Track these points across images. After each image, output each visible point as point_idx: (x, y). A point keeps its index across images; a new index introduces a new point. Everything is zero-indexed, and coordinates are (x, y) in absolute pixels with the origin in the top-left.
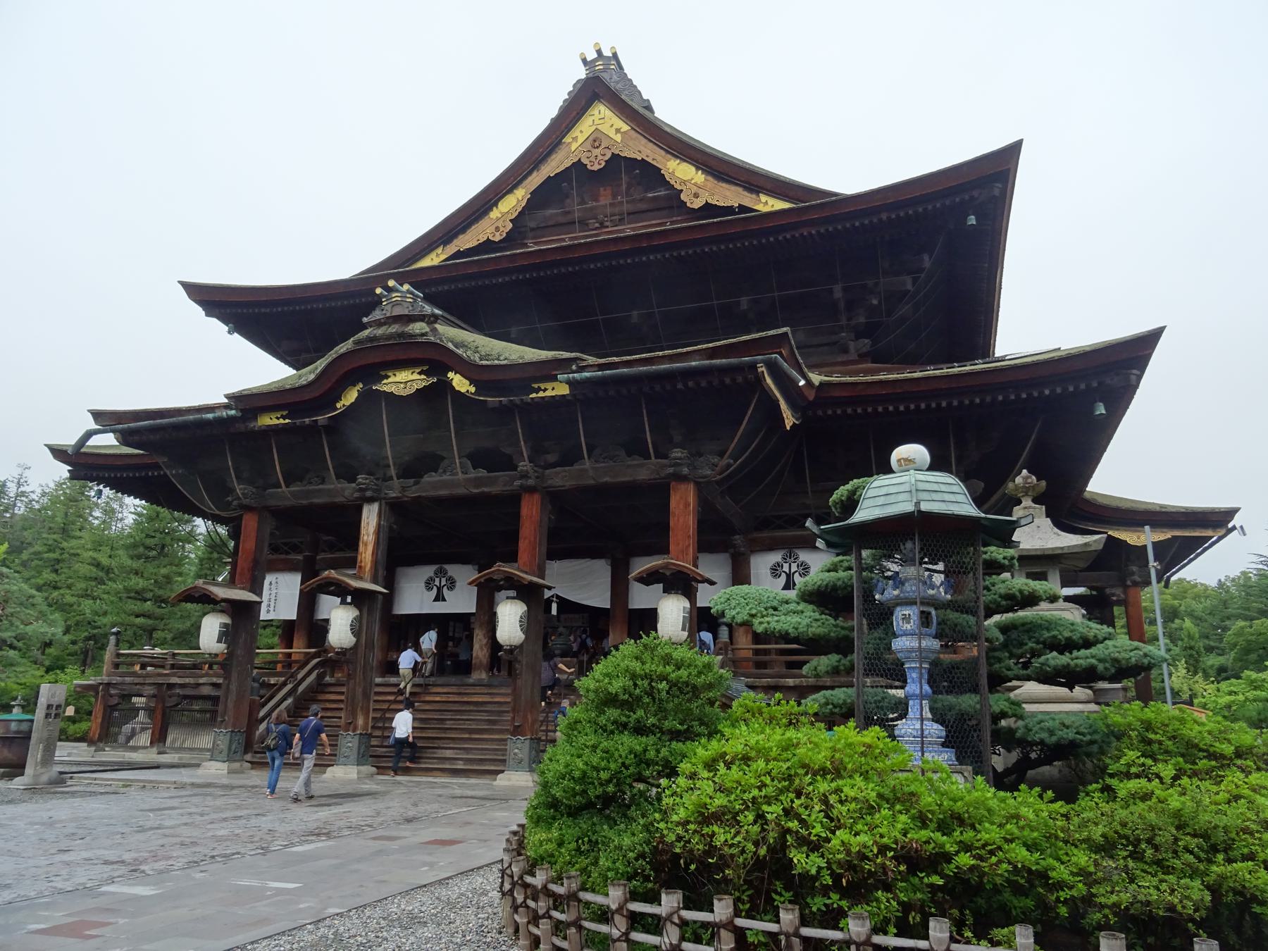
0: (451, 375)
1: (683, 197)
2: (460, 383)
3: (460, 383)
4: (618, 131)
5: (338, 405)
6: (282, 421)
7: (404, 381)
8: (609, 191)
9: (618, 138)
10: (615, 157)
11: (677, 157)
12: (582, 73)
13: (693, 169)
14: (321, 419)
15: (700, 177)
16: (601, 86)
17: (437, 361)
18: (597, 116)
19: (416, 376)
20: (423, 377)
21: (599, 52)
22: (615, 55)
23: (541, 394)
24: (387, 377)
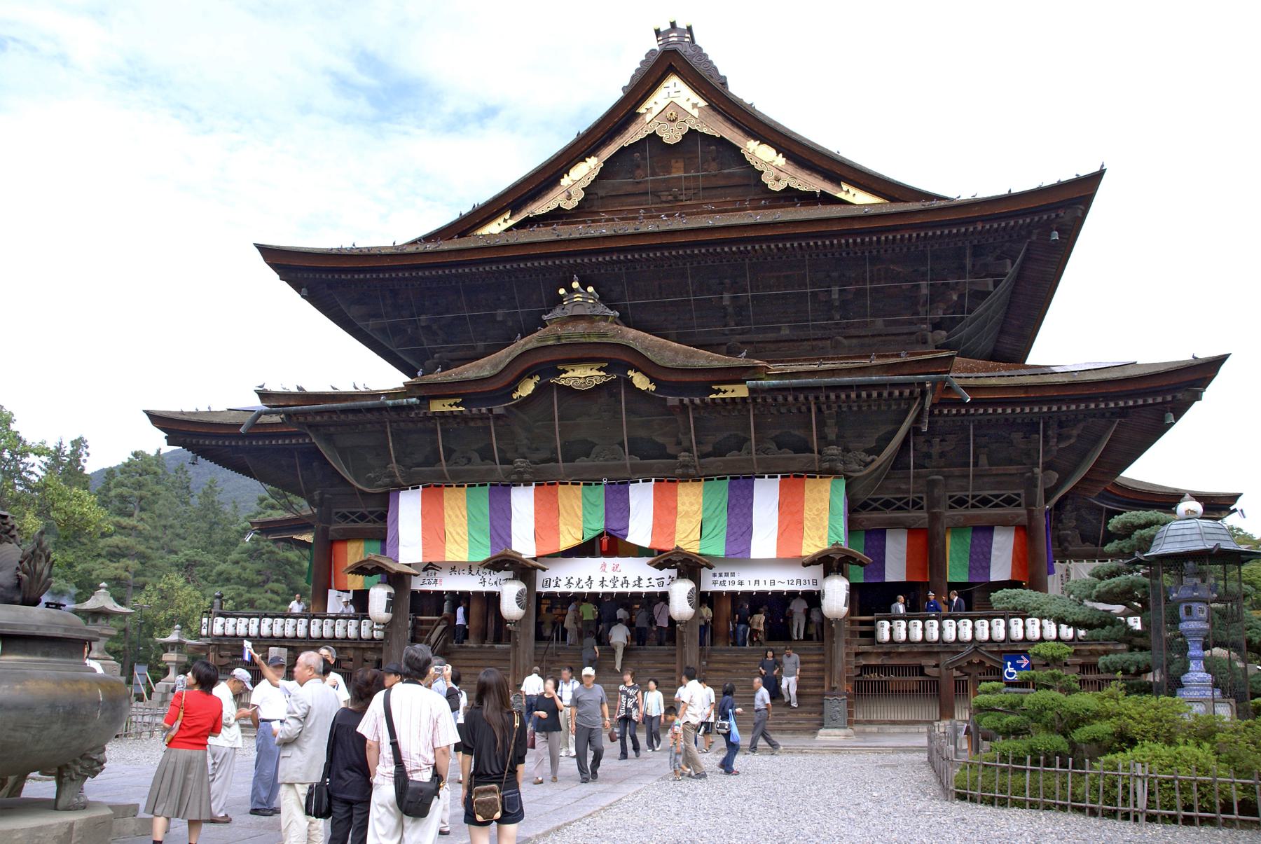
0: (631, 373)
1: (764, 178)
2: (641, 381)
3: (641, 381)
4: (695, 105)
5: (515, 396)
6: (454, 409)
7: (581, 376)
8: (681, 165)
9: (695, 113)
10: (692, 132)
11: (756, 139)
12: (654, 44)
13: (774, 152)
14: (498, 409)
15: (781, 161)
16: (674, 59)
17: (619, 361)
18: (672, 89)
19: (598, 373)
20: (602, 373)
21: (673, 24)
22: (689, 29)
23: (721, 395)
24: (566, 372)
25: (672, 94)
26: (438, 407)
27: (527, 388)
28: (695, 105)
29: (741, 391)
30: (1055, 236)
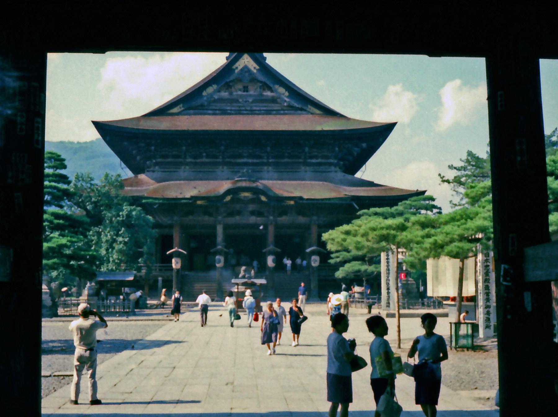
2: (263, 198)
3: (263, 198)
4: (255, 68)
9: (255, 71)
17: (256, 191)
18: (246, 60)
25: (246, 63)
26: (199, 202)
27: (228, 198)
28: (255, 68)
29: (292, 203)
30: (381, 140)
